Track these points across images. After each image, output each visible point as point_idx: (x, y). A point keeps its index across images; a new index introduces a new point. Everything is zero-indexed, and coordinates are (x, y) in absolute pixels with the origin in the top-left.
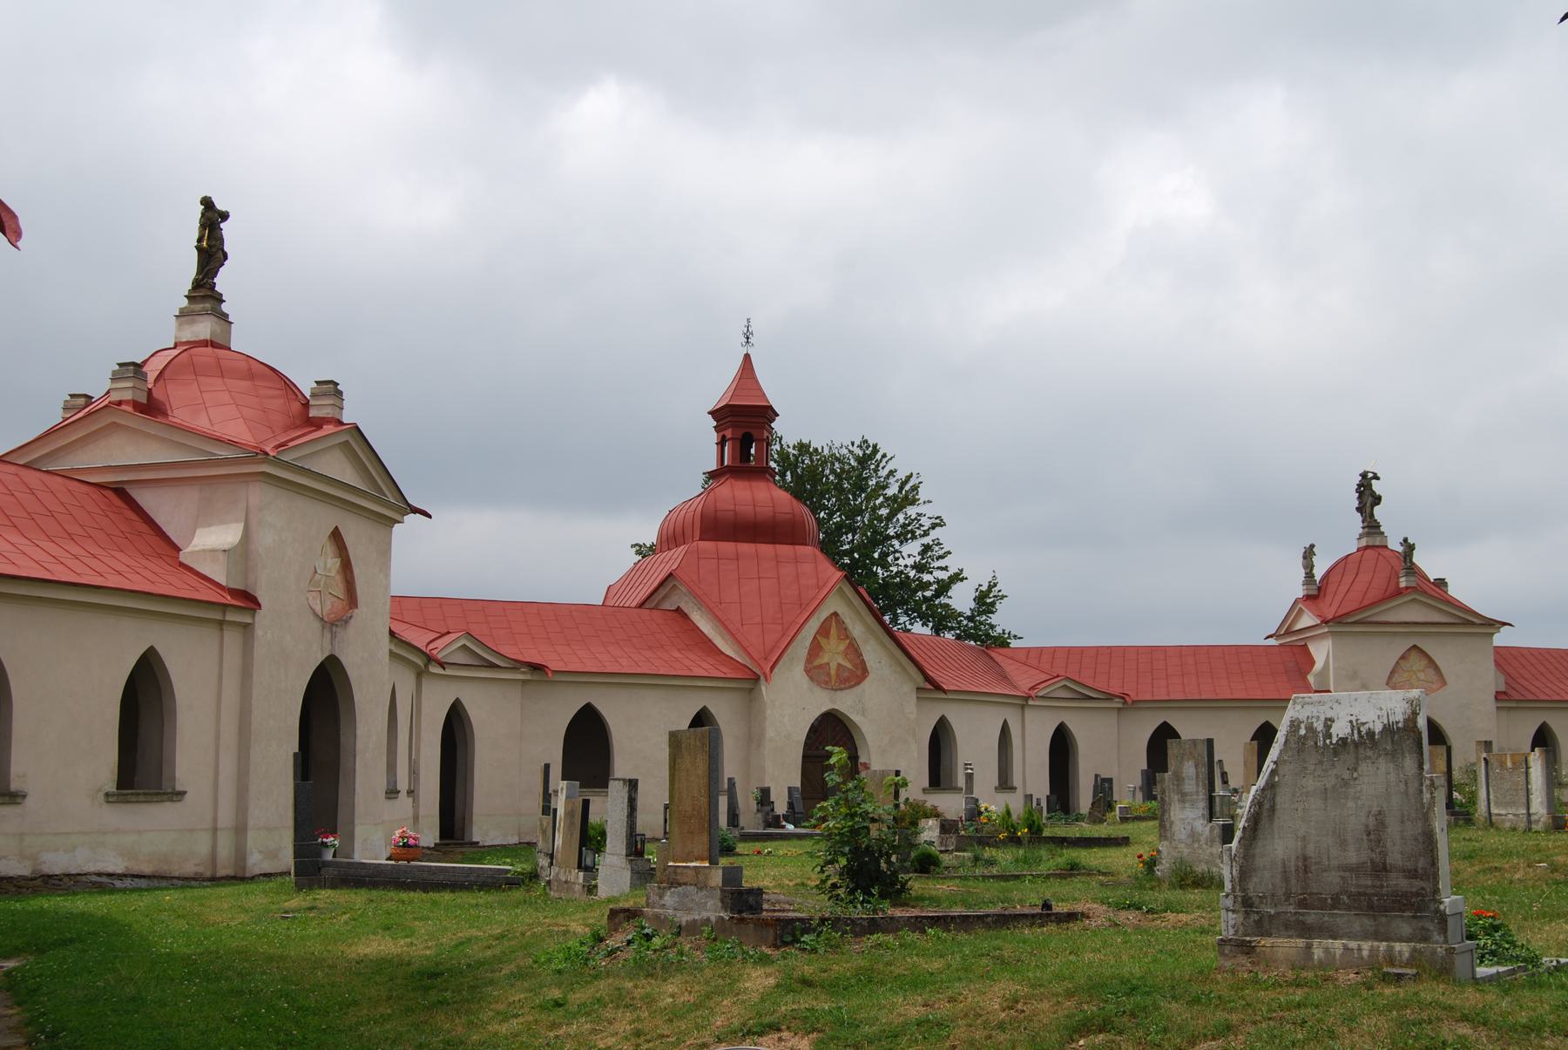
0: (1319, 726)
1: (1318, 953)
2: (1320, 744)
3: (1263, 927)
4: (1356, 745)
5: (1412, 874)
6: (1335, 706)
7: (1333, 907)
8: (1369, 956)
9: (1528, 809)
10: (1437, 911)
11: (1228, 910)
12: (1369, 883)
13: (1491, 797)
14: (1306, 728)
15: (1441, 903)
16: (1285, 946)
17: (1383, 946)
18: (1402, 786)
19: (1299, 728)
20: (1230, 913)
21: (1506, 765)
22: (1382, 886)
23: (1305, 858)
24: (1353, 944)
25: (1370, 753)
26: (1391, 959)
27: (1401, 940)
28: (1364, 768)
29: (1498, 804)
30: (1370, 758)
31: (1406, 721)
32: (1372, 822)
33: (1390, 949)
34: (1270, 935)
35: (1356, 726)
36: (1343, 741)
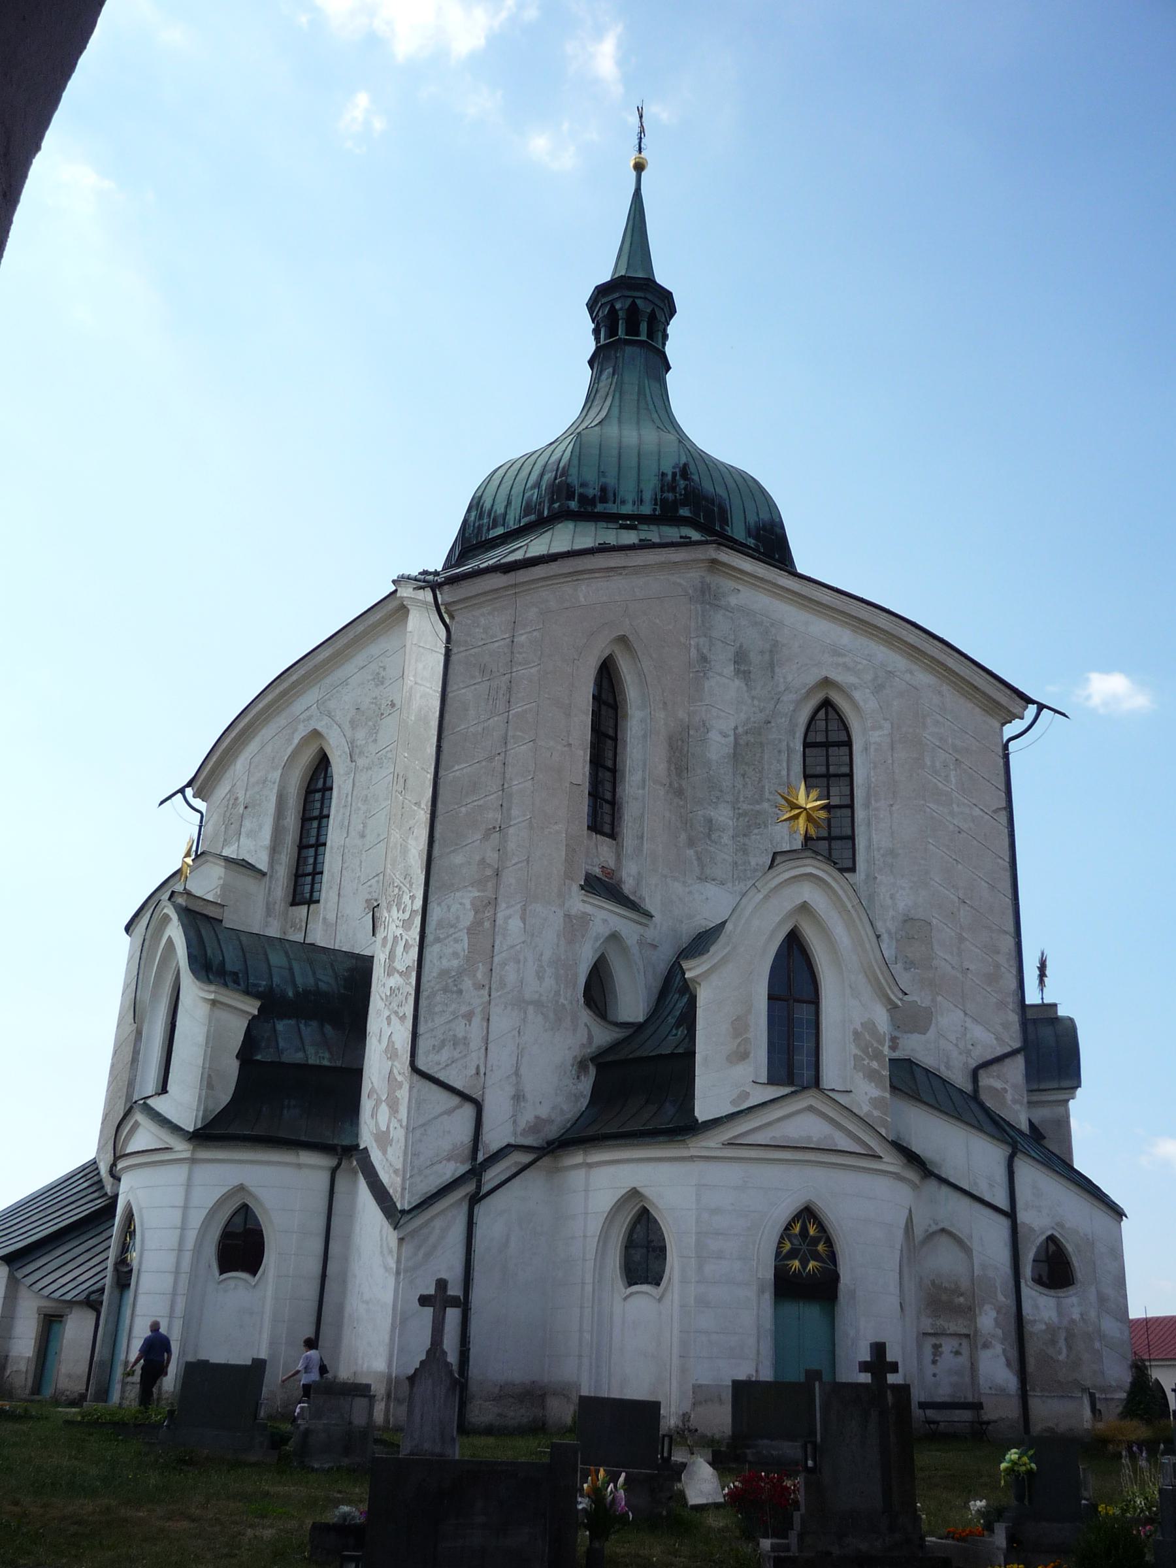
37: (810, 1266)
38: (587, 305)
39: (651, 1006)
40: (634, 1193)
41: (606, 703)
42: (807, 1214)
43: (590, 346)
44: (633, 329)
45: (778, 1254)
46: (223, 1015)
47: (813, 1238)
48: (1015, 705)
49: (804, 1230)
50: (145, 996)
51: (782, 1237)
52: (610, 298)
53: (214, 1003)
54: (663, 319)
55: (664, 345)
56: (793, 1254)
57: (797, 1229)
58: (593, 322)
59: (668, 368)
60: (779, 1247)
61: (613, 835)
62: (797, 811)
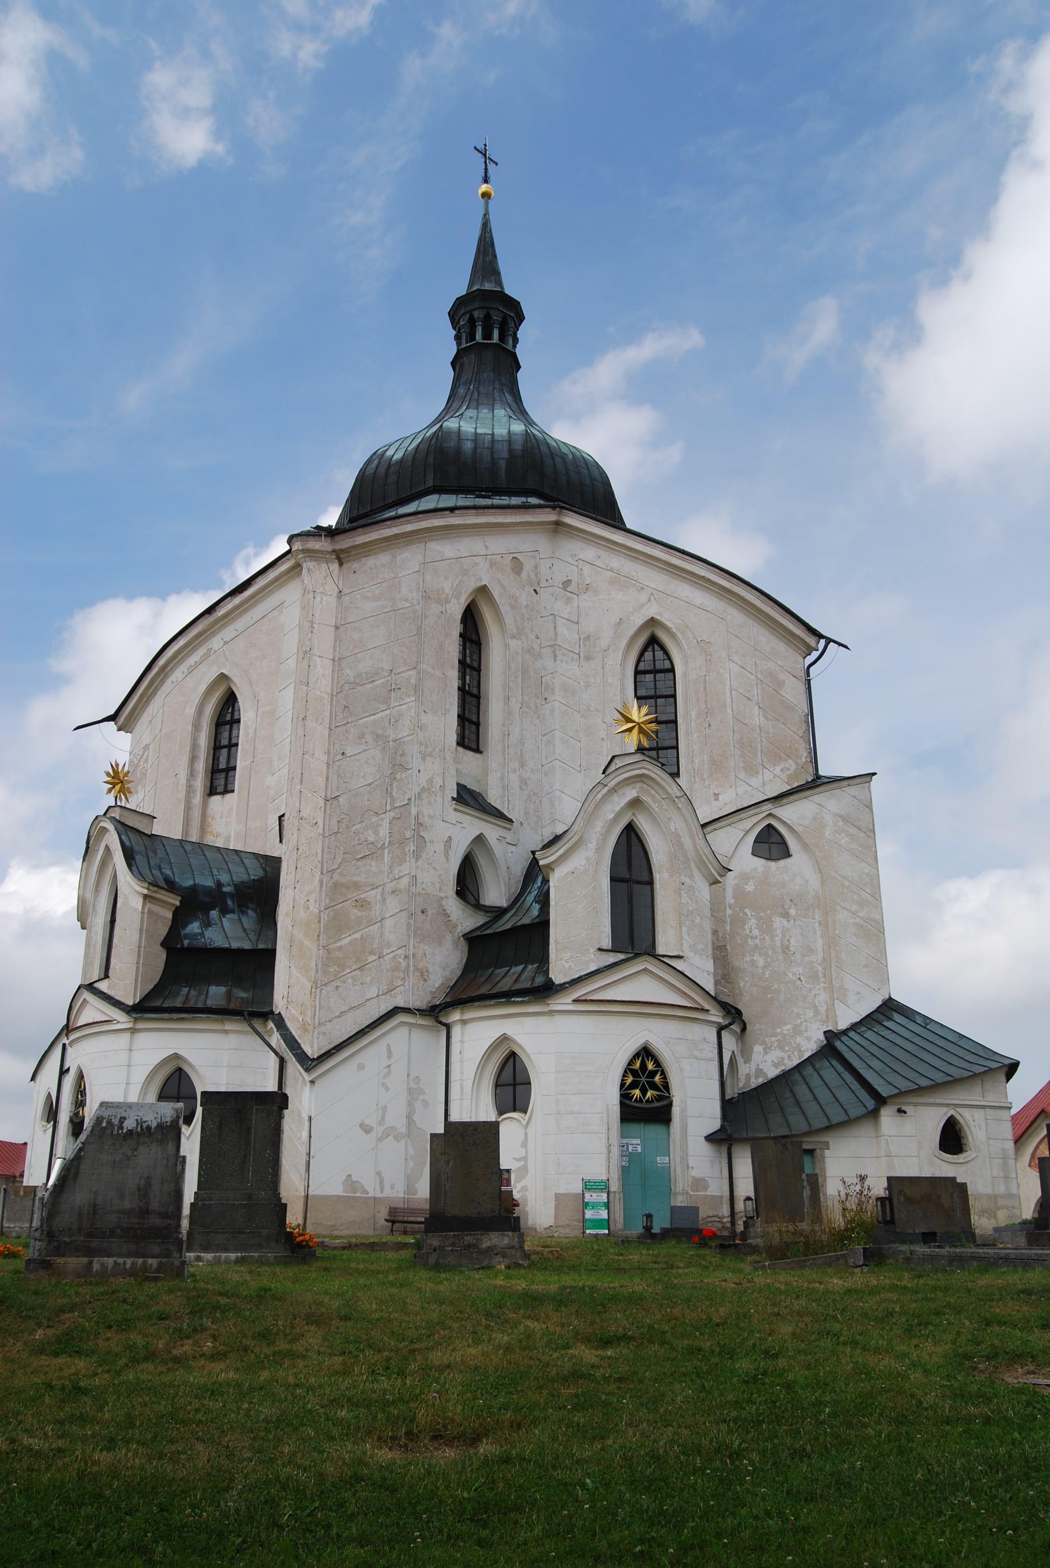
0: (116, 1122)
1: (96, 1267)
2: (115, 1133)
3: (60, 1250)
4: (139, 1135)
5: (164, 1215)
6: (128, 1109)
7: (110, 1237)
8: (130, 1268)
9: (31, 1223)
10: (178, 1238)
11: (36, 1239)
12: (136, 1221)
13: (5, 1215)
14: (107, 1122)
15: (181, 1233)
16: (73, 1262)
17: (140, 1261)
18: (165, 1161)
19: (102, 1122)
20: (37, 1242)
21: (19, 1192)
22: (144, 1223)
23: (95, 1205)
24: (121, 1260)
25: (146, 1140)
26: (145, 1268)
27: (153, 1257)
28: (142, 1149)
29: (8, 1220)
30: (146, 1143)
31: (172, 1121)
32: (142, 1182)
33: (145, 1263)
34: (64, 1256)
35: (140, 1122)
36: (130, 1132)
37: (649, 1094)
38: (449, 313)
39: (513, 890)
40: (504, 1039)
41: (472, 641)
42: (645, 1053)
43: (451, 349)
44: (488, 335)
45: (622, 1085)
46: (155, 908)
47: (651, 1072)
48: (811, 640)
49: (643, 1066)
50: (89, 895)
51: (625, 1071)
52: (469, 308)
53: (146, 897)
54: (513, 325)
55: (515, 347)
56: (634, 1085)
57: (637, 1065)
58: (454, 328)
59: (518, 367)
60: (622, 1080)
61: (477, 750)
62: (630, 725)
